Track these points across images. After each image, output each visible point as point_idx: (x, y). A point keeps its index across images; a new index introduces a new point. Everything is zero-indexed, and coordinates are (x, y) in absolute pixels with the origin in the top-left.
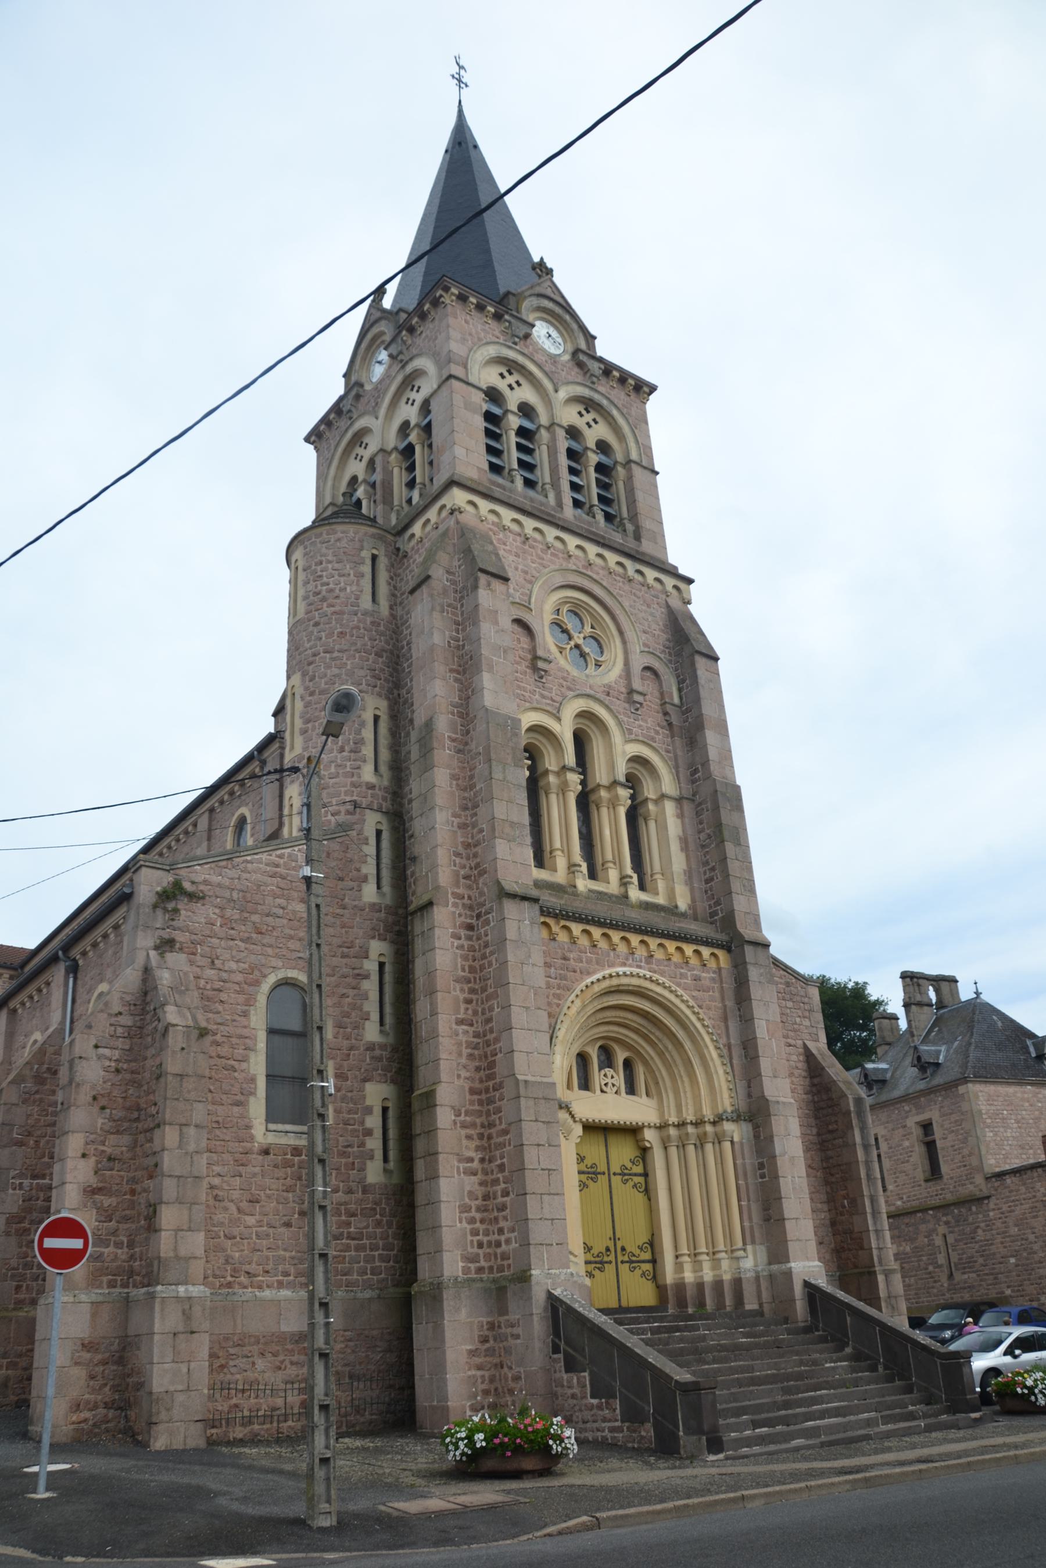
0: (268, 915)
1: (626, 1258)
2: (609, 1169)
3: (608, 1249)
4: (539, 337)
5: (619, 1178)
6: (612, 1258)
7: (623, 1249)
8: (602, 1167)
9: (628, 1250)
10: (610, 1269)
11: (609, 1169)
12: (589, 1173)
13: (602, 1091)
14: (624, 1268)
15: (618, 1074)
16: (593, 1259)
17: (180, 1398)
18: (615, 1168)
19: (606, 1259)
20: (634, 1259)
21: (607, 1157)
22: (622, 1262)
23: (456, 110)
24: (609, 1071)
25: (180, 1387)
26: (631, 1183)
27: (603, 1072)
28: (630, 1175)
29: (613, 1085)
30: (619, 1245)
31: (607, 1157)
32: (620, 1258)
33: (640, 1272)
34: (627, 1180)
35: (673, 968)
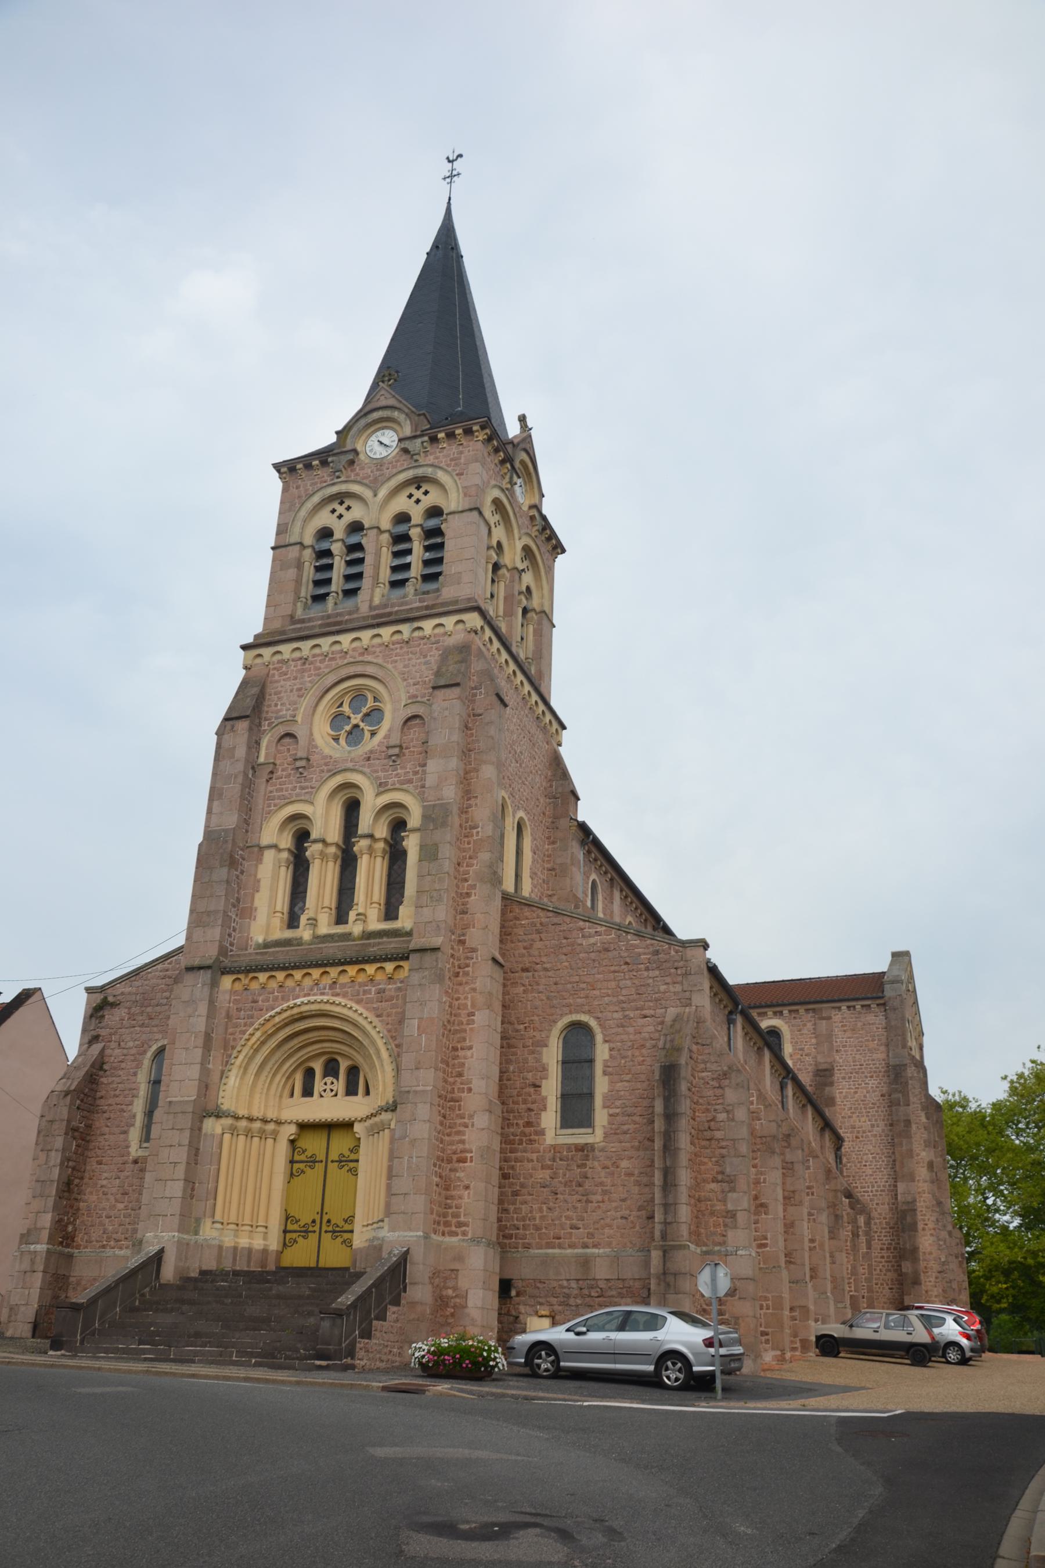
0: (157, 1005)
1: (330, 1229)
2: (327, 1158)
3: (314, 1221)
4: (383, 434)
5: (336, 1164)
6: (317, 1228)
7: (329, 1221)
8: (321, 1156)
9: (333, 1222)
10: (313, 1238)
11: (327, 1158)
12: (307, 1162)
13: (322, 1096)
14: (327, 1238)
15: (338, 1079)
16: (299, 1229)
17: (23, 1308)
18: (334, 1155)
19: (311, 1229)
20: (337, 1229)
21: (328, 1148)
22: (326, 1232)
23: (445, 205)
24: (329, 1080)
25: (23, 1303)
26: (346, 1168)
27: (324, 1081)
28: (346, 1161)
29: (332, 1090)
30: (325, 1218)
31: (328, 1148)
32: (324, 1228)
33: (342, 1240)
34: (343, 1166)
35: (357, 987)
